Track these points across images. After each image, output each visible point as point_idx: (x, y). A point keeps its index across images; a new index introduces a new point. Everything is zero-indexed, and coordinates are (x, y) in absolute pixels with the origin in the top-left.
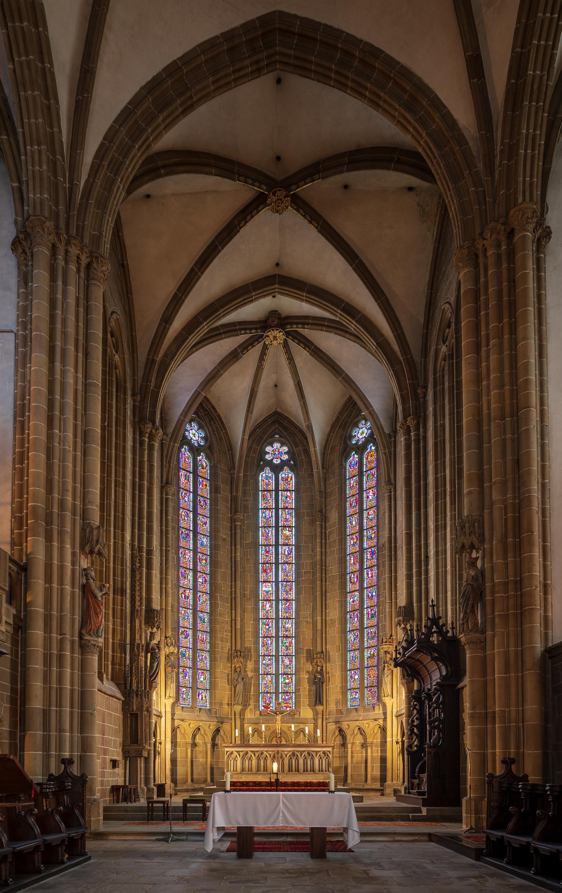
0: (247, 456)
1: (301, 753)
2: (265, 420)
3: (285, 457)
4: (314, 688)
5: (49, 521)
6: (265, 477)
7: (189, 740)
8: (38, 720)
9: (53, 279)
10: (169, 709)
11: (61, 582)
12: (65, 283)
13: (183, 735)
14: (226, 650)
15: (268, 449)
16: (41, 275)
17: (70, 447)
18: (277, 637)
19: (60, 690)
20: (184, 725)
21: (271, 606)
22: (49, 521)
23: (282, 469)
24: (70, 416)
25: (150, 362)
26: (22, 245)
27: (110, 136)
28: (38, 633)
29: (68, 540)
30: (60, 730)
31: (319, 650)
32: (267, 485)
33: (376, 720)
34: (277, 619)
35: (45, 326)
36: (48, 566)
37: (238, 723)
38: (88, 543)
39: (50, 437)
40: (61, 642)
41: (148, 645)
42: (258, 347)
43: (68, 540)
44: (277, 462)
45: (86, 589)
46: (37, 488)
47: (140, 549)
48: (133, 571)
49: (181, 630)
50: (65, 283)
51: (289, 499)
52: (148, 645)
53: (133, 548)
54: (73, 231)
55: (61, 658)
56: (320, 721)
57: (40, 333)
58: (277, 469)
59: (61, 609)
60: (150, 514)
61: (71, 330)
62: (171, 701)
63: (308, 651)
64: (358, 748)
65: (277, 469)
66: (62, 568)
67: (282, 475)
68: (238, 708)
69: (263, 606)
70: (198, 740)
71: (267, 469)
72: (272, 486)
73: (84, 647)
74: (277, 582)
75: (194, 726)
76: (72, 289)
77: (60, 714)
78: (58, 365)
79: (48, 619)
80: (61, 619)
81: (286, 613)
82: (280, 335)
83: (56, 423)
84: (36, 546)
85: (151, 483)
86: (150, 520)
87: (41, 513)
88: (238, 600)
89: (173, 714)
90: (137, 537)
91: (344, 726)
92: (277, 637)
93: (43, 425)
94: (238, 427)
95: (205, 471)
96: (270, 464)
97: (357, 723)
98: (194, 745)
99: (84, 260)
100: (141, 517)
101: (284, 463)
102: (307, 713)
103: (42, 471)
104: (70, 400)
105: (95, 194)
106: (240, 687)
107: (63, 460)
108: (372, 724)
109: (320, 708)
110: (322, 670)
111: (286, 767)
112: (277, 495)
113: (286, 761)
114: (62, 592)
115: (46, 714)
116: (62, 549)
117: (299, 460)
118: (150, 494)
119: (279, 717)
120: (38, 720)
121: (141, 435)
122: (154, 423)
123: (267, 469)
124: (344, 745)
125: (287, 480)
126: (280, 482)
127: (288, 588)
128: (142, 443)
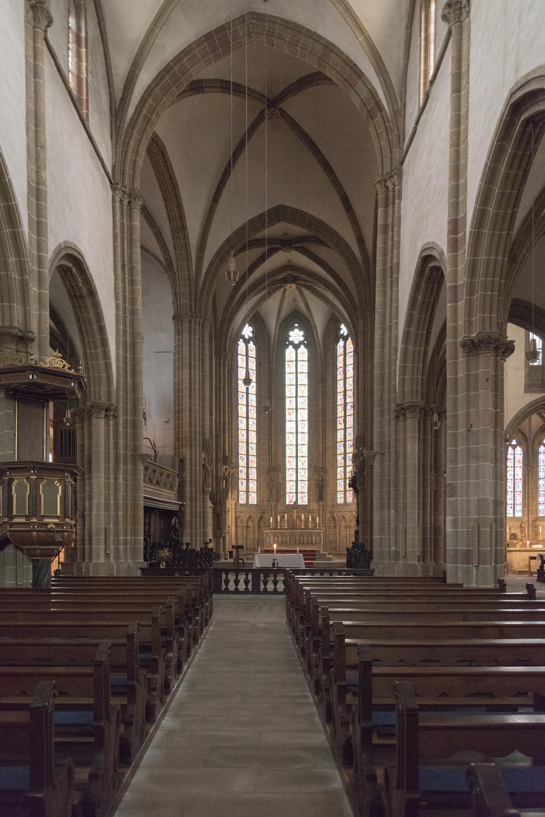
0: (278, 340)
1: (306, 533)
2: (289, 315)
3: (302, 339)
4: (318, 490)
5: (191, 441)
6: (290, 352)
7: (245, 525)
8: (188, 524)
9: (190, 334)
10: (233, 507)
11: (196, 466)
12: (195, 335)
13: (241, 521)
14: (266, 467)
15: (291, 333)
16: (186, 334)
17: (197, 407)
18: (297, 457)
19: (196, 512)
20: (242, 515)
21: (293, 437)
22: (191, 441)
23: (299, 347)
24: (197, 394)
25: (224, 319)
26: (177, 318)
27: (211, 265)
28: (188, 489)
29: (198, 447)
30: (196, 529)
31: (321, 466)
32: (291, 357)
33: (351, 512)
34: (297, 445)
35: (188, 358)
36: (191, 459)
37: (273, 513)
38: (205, 447)
39: (190, 403)
40: (196, 492)
41: (224, 475)
42: (282, 290)
43: (198, 447)
44: (296, 342)
45: (204, 466)
46: (186, 428)
47: (220, 423)
48: (216, 436)
49: (240, 456)
50: (195, 335)
51: (304, 367)
52: (224, 475)
53: (216, 423)
54: (197, 311)
55: (196, 498)
56: (321, 511)
57: (186, 361)
58: (296, 347)
59: (195, 478)
60: (224, 402)
61: (197, 356)
62: (235, 501)
63: (315, 466)
64: (343, 529)
65: (296, 347)
66: (196, 460)
67: (299, 350)
68: (273, 503)
69: (288, 437)
70: (250, 524)
71: (291, 347)
72: (294, 359)
73: (204, 492)
74: (297, 421)
75: (247, 516)
76: (197, 337)
77: (196, 521)
78: (193, 372)
79: (191, 482)
80: (196, 481)
81: (302, 441)
82: (294, 286)
83: (193, 397)
84: (186, 453)
85: (224, 385)
86: (224, 406)
87: (188, 438)
88: (273, 434)
89: (236, 509)
90: (218, 417)
91: (335, 515)
92: (297, 457)
93: (188, 400)
94: (272, 324)
95: (253, 353)
96: (292, 343)
97: (342, 513)
98: (248, 527)
99: (202, 321)
100: (220, 405)
101: (301, 343)
102: (315, 506)
103: (188, 420)
104: (197, 386)
105: (205, 291)
106: (274, 490)
107: (195, 413)
108: (349, 514)
109: (321, 503)
110: (323, 479)
111: (297, 542)
112: (297, 364)
113: (297, 538)
114: (196, 469)
115: (191, 522)
116: (195, 451)
117: (310, 342)
118: (224, 391)
119: (295, 511)
120: (188, 524)
121: (220, 360)
122: (226, 352)
123: (291, 347)
124: (335, 527)
125: (302, 354)
126: (299, 355)
127: (303, 426)
128: (220, 364)
